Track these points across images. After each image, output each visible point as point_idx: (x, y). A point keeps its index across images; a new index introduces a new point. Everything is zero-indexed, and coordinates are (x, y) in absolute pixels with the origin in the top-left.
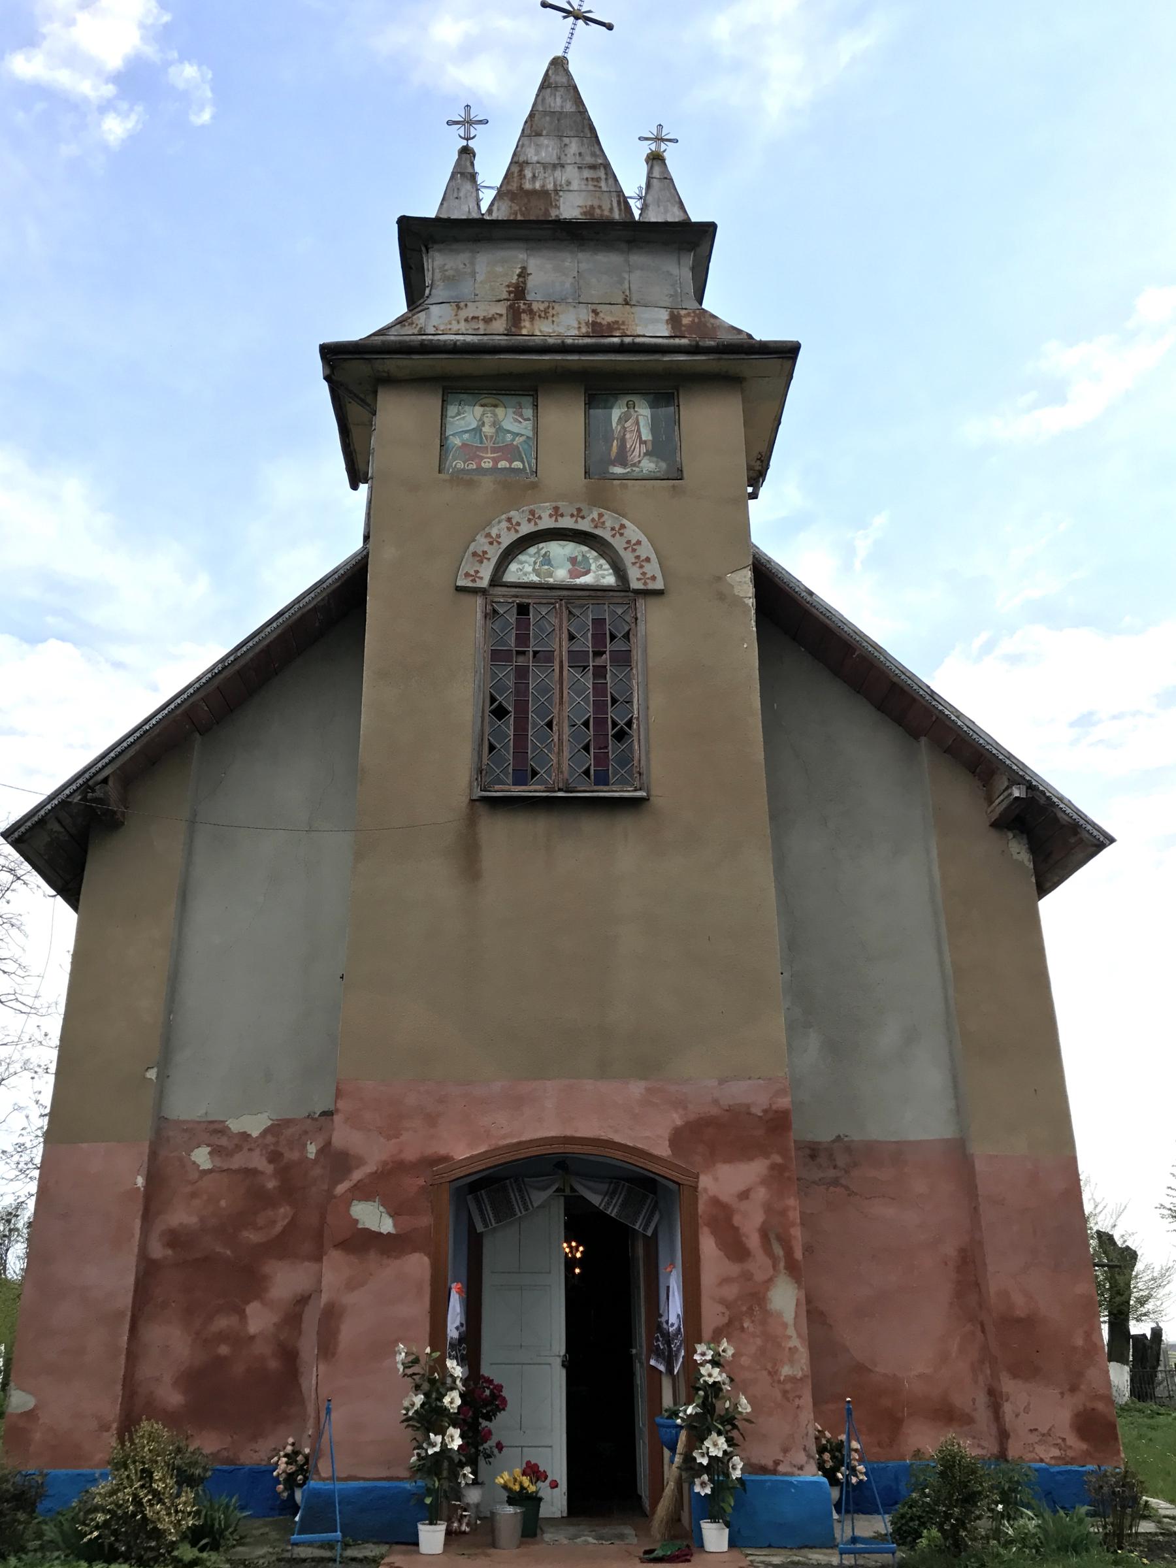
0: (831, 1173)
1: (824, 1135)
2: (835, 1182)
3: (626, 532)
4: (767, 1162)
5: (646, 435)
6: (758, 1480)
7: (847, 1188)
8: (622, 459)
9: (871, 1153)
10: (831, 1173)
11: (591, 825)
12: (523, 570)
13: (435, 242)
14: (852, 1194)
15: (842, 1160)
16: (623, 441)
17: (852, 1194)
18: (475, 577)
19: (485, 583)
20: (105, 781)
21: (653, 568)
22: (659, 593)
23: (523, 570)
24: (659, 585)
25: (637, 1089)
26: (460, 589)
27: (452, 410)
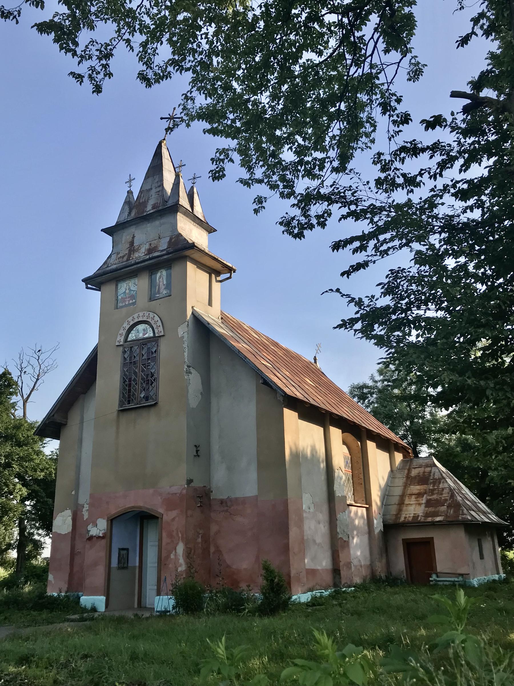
0: (226, 508)
1: (224, 497)
2: (227, 511)
3: (155, 318)
4: (420, 514)
5: (165, 283)
6: (135, 585)
7: (230, 513)
8: (159, 292)
9: (236, 501)
10: (226, 508)
11: (144, 413)
12: (132, 336)
13: (114, 233)
14: (231, 514)
15: (229, 504)
16: (159, 285)
17: (231, 514)
18: (119, 342)
19: (121, 343)
20: (53, 416)
21: (161, 329)
22: (163, 336)
23: (132, 336)
24: (162, 334)
25: (151, 491)
26: (118, 346)
27: (119, 285)
